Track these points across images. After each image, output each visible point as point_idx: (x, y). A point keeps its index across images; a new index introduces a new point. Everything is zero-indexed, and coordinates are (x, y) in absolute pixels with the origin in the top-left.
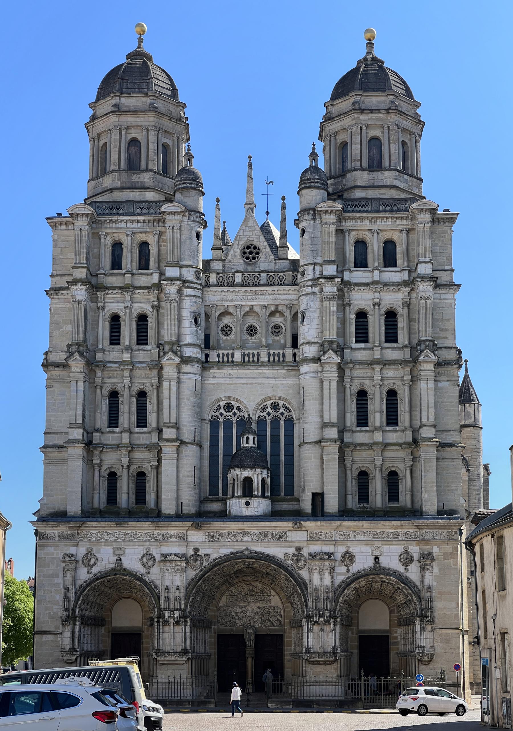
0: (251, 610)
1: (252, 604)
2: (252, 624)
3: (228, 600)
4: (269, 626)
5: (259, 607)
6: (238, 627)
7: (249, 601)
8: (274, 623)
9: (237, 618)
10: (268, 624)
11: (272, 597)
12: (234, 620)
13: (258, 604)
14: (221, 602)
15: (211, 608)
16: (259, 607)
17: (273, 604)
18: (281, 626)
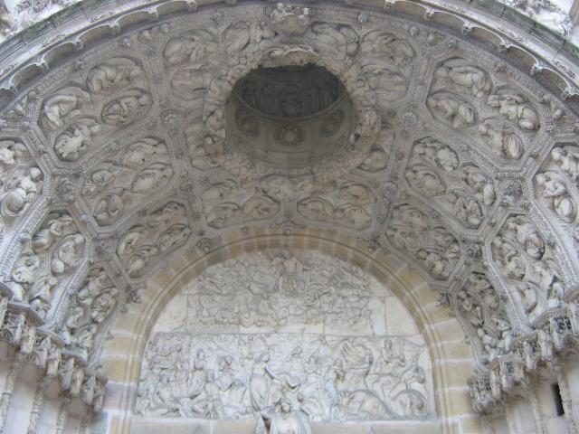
0: (288, 348)
1: (295, 328)
2: (296, 405)
3: (192, 313)
4: (372, 417)
5: (322, 338)
6: (228, 418)
7: (281, 313)
8: (396, 407)
9: (227, 380)
10: (369, 405)
11: (374, 304)
12: (211, 388)
13: (319, 329)
14: (164, 317)
15: (114, 332)
16: (322, 338)
17: (379, 329)
18: (427, 417)
